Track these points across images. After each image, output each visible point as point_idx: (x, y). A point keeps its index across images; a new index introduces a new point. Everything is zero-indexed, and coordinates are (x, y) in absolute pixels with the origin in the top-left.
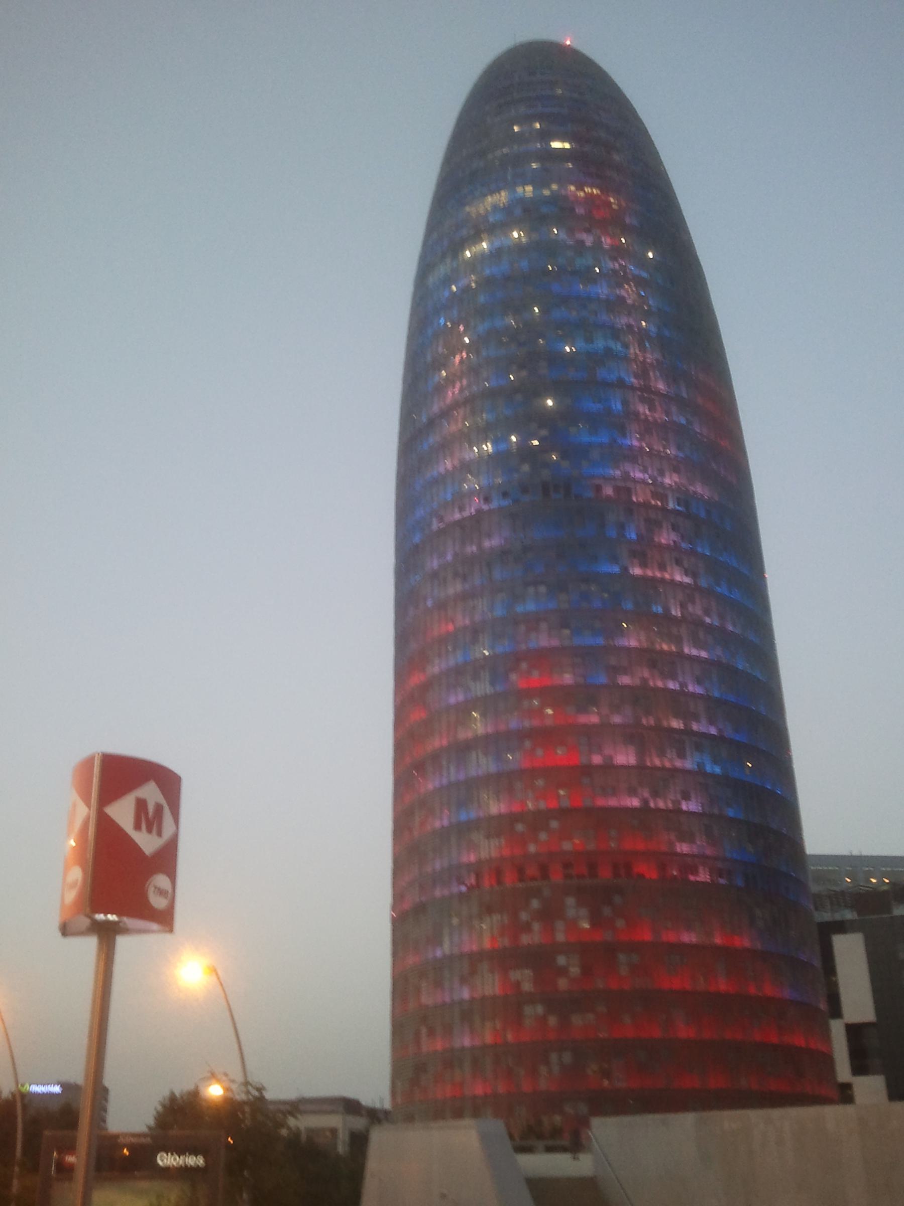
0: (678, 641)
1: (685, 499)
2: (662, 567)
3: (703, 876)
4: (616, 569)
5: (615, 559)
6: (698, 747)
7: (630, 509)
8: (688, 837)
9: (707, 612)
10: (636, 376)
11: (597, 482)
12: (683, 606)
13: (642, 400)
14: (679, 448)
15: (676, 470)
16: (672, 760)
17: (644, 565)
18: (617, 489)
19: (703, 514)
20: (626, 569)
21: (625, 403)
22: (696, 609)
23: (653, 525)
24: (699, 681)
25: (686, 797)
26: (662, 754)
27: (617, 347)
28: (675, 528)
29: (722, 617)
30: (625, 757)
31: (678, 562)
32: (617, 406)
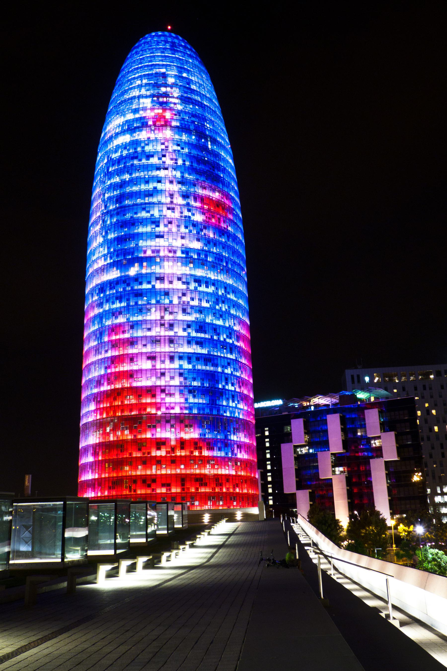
2: (171, 282)
3: (177, 410)
4: (149, 286)
5: (149, 282)
6: (181, 358)
8: (170, 395)
9: (192, 299)
11: (144, 249)
12: (179, 298)
13: (169, 209)
14: (186, 227)
16: (168, 365)
18: (153, 252)
19: (196, 257)
20: (154, 286)
22: (186, 299)
24: (184, 330)
25: (172, 378)
26: (163, 362)
27: (159, 186)
29: (200, 300)
30: (147, 365)
31: (179, 279)
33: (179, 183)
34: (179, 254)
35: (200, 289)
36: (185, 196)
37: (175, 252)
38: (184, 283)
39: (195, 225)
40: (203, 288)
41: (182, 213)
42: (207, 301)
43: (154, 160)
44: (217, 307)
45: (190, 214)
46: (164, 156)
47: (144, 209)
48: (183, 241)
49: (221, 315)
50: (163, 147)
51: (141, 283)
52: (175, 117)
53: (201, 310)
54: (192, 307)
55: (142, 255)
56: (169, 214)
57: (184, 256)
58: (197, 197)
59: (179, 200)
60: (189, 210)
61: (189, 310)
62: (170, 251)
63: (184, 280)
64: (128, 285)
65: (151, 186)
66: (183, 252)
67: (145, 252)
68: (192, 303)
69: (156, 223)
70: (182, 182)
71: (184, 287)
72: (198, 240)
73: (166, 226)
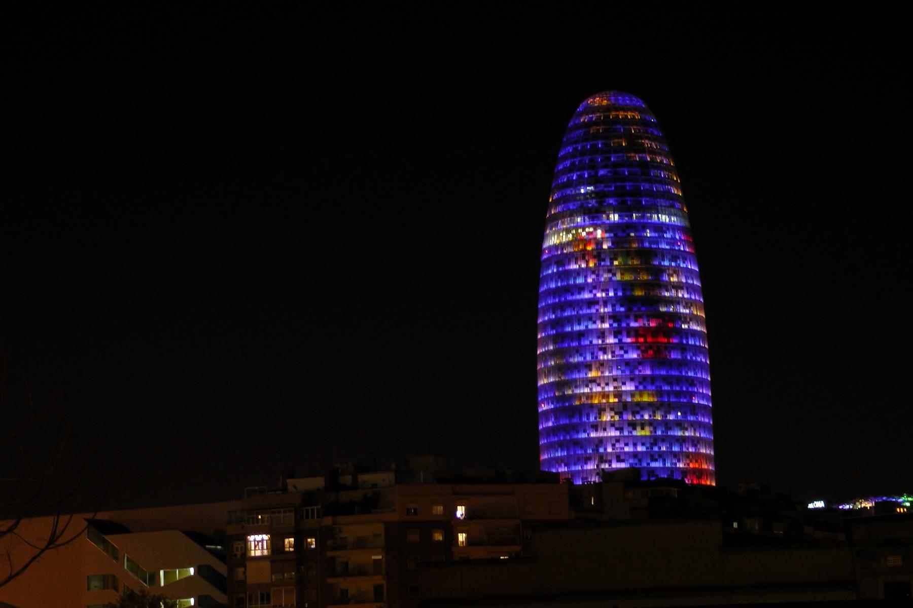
0: (610, 462)
1: (618, 394)
2: (605, 430)
5: (585, 431)
7: (592, 406)
9: (626, 445)
10: (599, 338)
12: (613, 445)
13: (600, 349)
15: (615, 380)
17: (597, 430)
18: (587, 398)
21: (592, 354)
23: (601, 410)
28: (612, 409)
29: (635, 445)
32: (589, 358)
33: (610, 317)
34: (612, 400)
35: (635, 433)
36: (616, 333)
37: (608, 397)
38: (617, 429)
39: (628, 363)
40: (638, 433)
41: (613, 352)
42: (643, 444)
43: (587, 296)
44: (656, 449)
45: (622, 352)
46: (595, 288)
47: (577, 352)
48: (616, 384)
49: (661, 456)
50: (594, 276)
51: (578, 432)
52: (607, 235)
53: (635, 455)
54: (628, 453)
55: (577, 403)
56: (602, 357)
57: (616, 400)
58: (630, 332)
59: (611, 340)
60: (621, 348)
61: (622, 457)
62: (603, 397)
63: (617, 426)
64: (568, 433)
65: (582, 327)
66: (615, 397)
67: (580, 399)
68: (627, 449)
69: (589, 367)
70: (614, 317)
71: (618, 433)
72: (632, 380)
73: (598, 369)
